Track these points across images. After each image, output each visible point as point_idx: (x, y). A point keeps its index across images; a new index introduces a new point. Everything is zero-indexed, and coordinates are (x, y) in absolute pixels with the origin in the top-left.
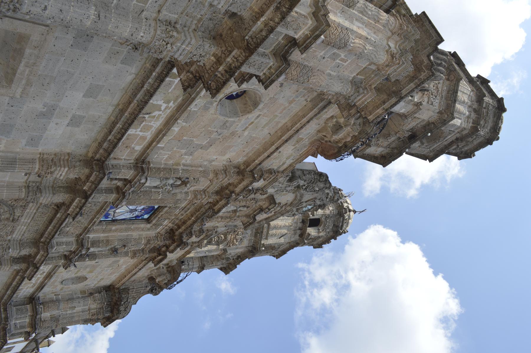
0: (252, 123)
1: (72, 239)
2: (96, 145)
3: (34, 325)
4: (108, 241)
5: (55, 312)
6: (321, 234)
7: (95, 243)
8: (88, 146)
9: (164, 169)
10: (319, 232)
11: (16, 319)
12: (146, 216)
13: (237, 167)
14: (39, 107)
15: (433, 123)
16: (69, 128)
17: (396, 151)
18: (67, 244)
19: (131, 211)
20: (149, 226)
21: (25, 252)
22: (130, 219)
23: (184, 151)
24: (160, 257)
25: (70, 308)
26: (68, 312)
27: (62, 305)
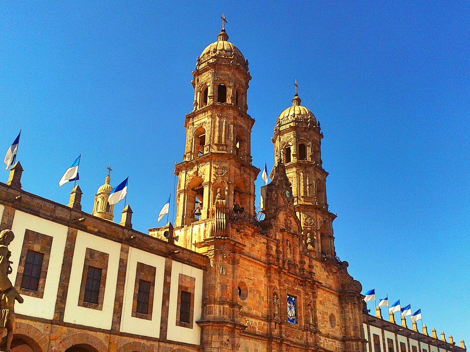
0: (249, 279)
1: (305, 333)
3: (357, 340)
5: (351, 328)
7: (307, 322)
9: (270, 308)
11: (353, 349)
12: (293, 299)
13: (267, 271)
17: (252, 169)
18: (307, 336)
19: (291, 309)
20: (298, 297)
22: (295, 307)
23: (262, 302)
25: (349, 320)
27: (348, 325)
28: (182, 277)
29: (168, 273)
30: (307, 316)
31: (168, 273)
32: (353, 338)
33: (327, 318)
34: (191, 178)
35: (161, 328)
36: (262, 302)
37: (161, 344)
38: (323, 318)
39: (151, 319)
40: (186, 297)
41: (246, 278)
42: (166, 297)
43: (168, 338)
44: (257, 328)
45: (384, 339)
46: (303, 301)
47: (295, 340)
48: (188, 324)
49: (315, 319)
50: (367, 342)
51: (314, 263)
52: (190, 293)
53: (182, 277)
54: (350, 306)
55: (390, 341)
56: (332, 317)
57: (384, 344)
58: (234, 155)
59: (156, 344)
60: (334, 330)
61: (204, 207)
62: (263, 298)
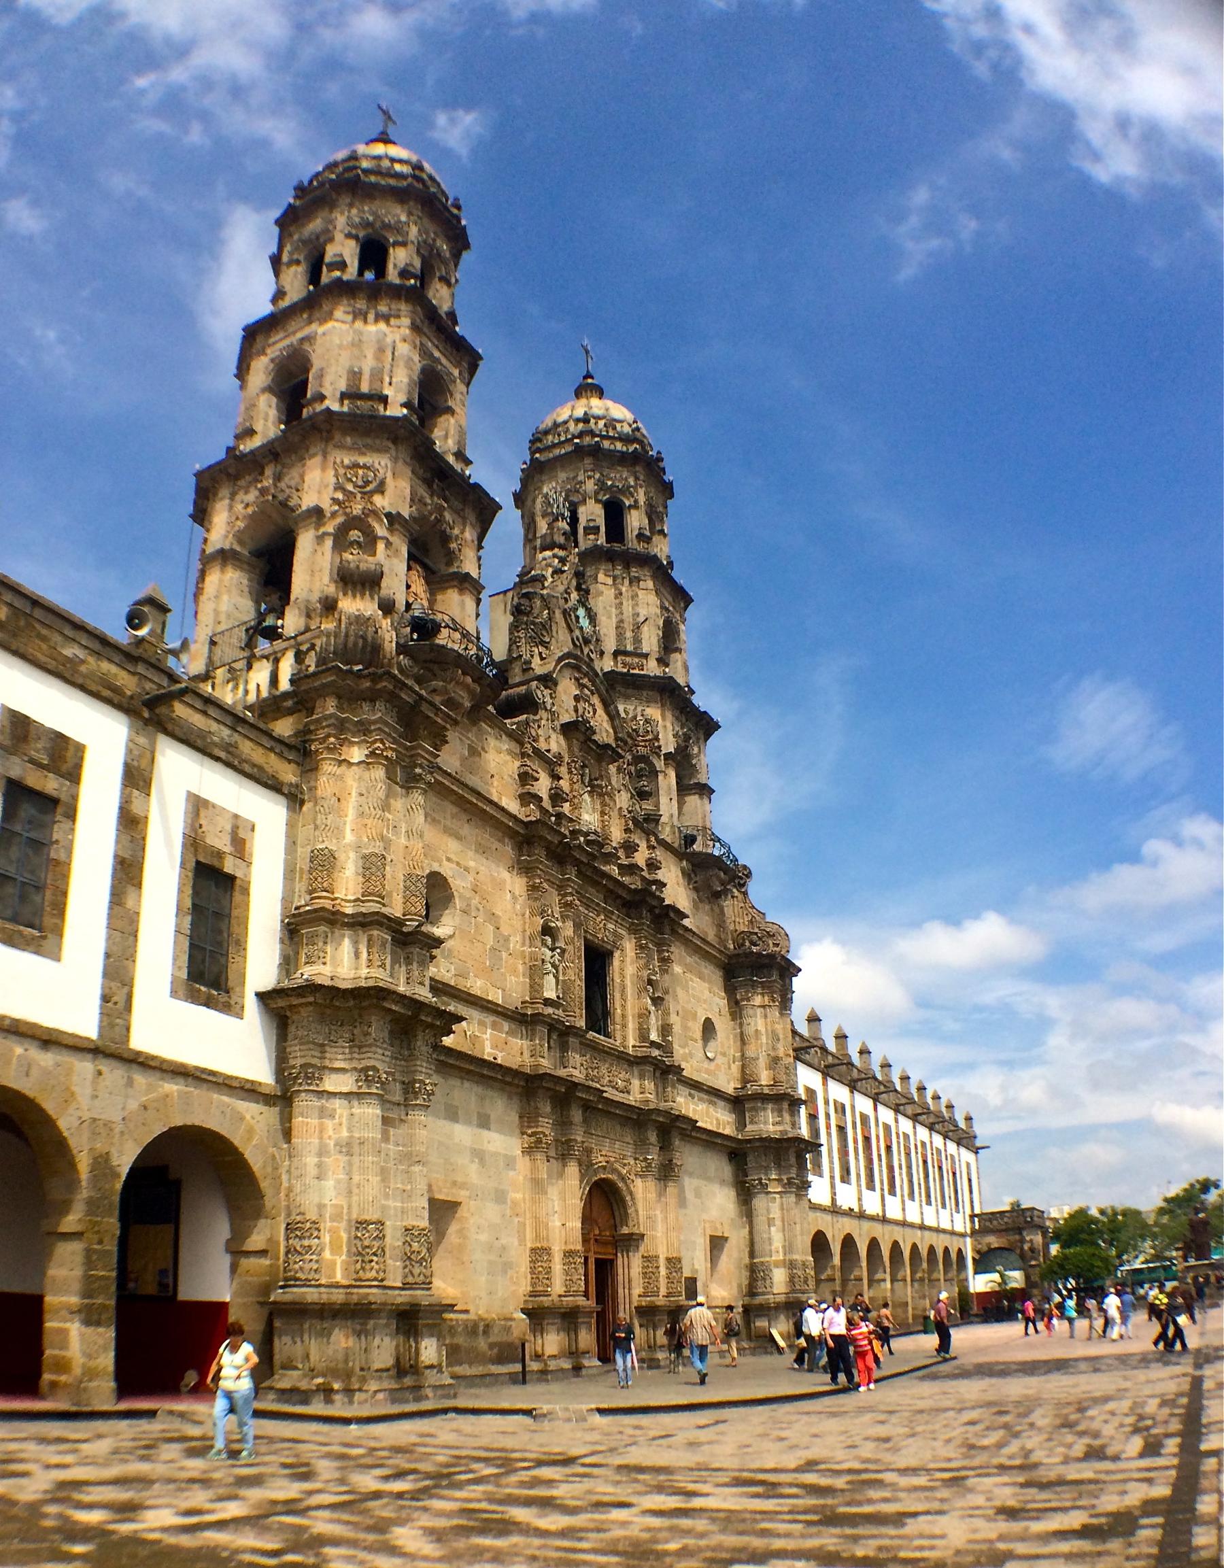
0: (458, 864)
2: (508, 1088)
4: (640, 1016)
5: (762, 1062)
6: (642, 499)
7: (643, 1035)
8: (510, 1098)
9: (531, 978)
10: (635, 506)
14: (474, 1167)
15: (415, 448)
16: (492, 1126)
17: (471, 497)
21: (653, 1137)
24: (672, 915)
26: (764, 1041)
27: (750, 1053)
28: (198, 805)
29: (137, 777)
30: (643, 1016)
31: (137, 777)
32: (766, 1091)
33: (697, 1030)
34: (250, 510)
35: (105, 999)
36: (504, 955)
37: (105, 1066)
38: (685, 1028)
39: (55, 955)
40: (213, 887)
41: (449, 859)
42: (128, 872)
43: (140, 1041)
44: (488, 1043)
45: (827, 1102)
46: (630, 970)
47: (610, 1093)
48: (223, 998)
49: (666, 1030)
50: (805, 1102)
51: (659, 854)
52: (231, 879)
53: (198, 805)
54: (758, 1000)
55: (840, 1109)
56: (708, 1029)
57: (828, 1116)
58: (412, 423)
59: (84, 1067)
60: (712, 1066)
61: (293, 597)
62: (507, 940)
